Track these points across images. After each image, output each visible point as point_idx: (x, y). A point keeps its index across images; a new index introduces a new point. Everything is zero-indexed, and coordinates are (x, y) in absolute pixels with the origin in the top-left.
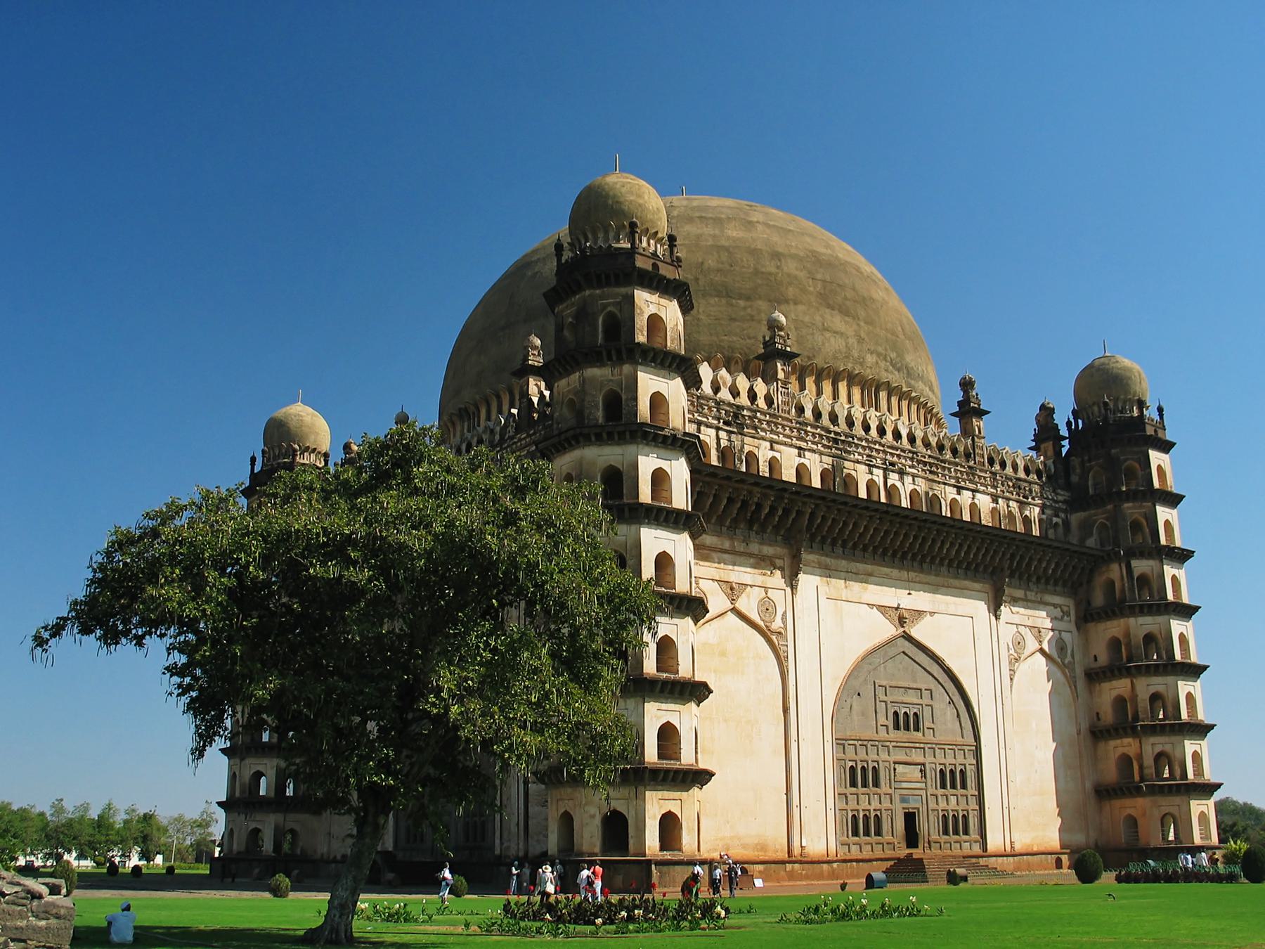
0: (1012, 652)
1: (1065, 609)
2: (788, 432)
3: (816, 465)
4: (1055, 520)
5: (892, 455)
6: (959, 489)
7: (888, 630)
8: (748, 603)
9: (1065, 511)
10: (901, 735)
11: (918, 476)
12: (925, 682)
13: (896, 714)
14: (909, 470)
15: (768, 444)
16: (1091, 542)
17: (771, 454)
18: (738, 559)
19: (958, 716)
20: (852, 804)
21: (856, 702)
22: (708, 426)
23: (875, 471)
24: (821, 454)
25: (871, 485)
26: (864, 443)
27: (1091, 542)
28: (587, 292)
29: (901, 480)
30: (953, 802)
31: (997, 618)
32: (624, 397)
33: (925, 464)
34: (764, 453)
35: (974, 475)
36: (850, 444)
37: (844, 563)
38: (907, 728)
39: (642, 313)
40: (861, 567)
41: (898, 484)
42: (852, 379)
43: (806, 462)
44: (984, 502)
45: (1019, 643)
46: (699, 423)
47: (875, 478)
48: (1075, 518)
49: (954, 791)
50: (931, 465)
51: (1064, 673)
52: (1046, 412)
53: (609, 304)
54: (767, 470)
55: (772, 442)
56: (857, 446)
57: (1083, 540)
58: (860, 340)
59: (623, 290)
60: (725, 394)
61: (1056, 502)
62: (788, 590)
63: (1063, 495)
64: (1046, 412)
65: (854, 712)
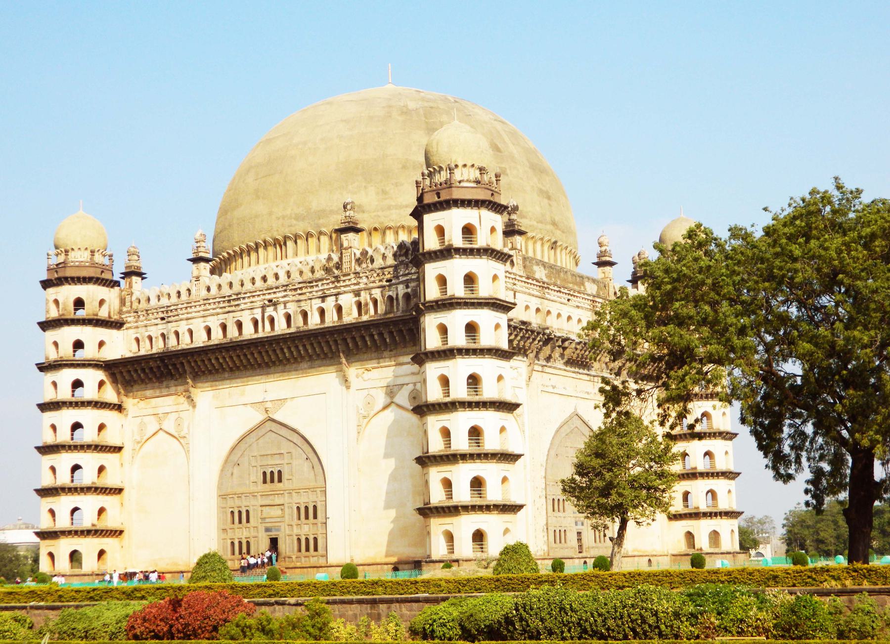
2: (198, 308)
3: (214, 323)
6: (323, 298)
8: (169, 424)
10: (269, 486)
11: (288, 302)
12: (285, 447)
13: (264, 473)
14: (281, 300)
15: (184, 322)
20: (230, 534)
21: (236, 470)
23: (255, 311)
26: (248, 295)
29: (276, 309)
30: (306, 529)
31: (348, 387)
33: (295, 290)
34: (183, 328)
35: (338, 282)
36: (238, 299)
41: (274, 314)
47: (256, 316)
49: (307, 521)
50: (301, 288)
55: (187, 319)
56: (244, 298)
58: (270, 214)
62: (191, 408)
65: (234, 476)
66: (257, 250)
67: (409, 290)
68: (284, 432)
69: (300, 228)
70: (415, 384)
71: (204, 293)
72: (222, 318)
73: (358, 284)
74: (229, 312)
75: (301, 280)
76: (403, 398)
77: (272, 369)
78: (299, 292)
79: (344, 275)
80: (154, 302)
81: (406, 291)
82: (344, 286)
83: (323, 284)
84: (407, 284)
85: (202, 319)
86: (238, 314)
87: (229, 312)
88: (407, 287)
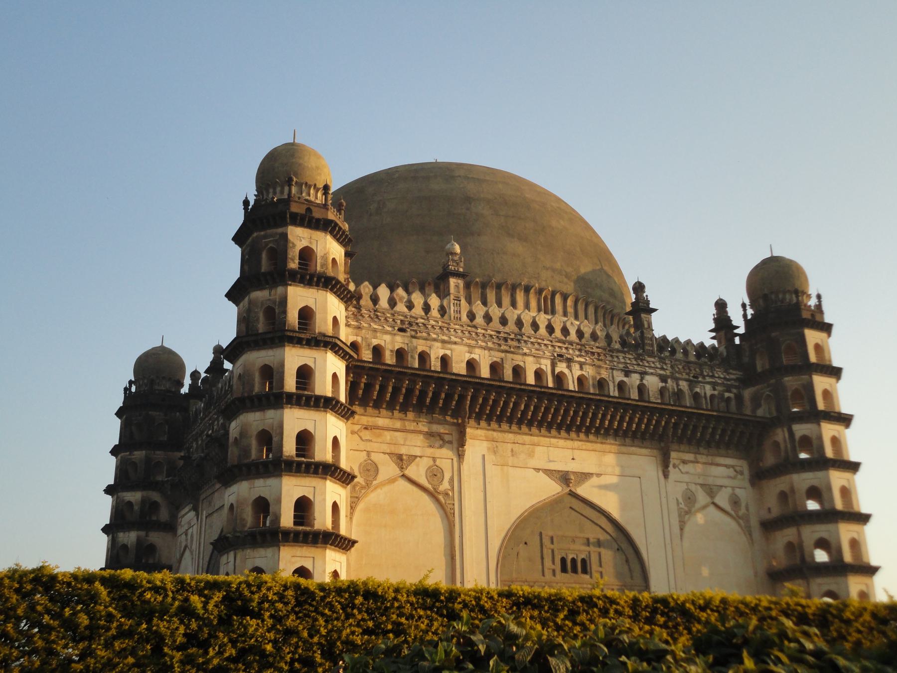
0: (682, 506)
1: (738, 469)
4: (727, 395)
5: (559, 347)
6: (627, 373)
7: (553, 488)
8: (418, 471)
9: (736, 387)
13: (563, 560)
15: (439, 344)
16: (760, 412)
17: (441, 352)
18: (410, 436)
19: (627, 561)
22: (387, 333)
23: (543, 361)
24: (490, 349)
25: (539, 374)
27: (760, 412)
28: (255, 234)
29: (569, 367)
31: (666, 476)
32: (277, 311)
33: (593, 353)
34: (436, 352)
35: (642, 360)
37: (511, 436)
38: (575, 570)
39: (294, 245)
40: (527, 438)
41: (566, 371)
42: (527, 290)
43: (476, 357)
44: (653, 382)
45: (690, 499)
46: (375, 331)
47: (543, 367)
48: (747, 393)
50: (598, 354)
51: (739, 524)
52: (721, 306)
53: (270, 242)
54: (439, 364)
55: (443, 342)
57: (754, 410)
59: (280, 230)
60: (401, 307)
61: (728, 380)
62: (455, 459)
63: (734, 375)
64: (721, 306)
66: (513, 289)
67: (716, 393)
68: (588, 512)
69: (569, 288)
70: (733, 488)
71: (464, 318)
72: (497, 356)
73: (662, 369)
74: (507, 352)
75: (597, 345)
76: (722, 499)
77: (573, 435)
78: (596, 356)
79: (650, 356)
80: (384, 303)
81: (713, 392)
82: (650, 367)
83: (624, 358)
84: (714, 385)
85: (466, 349)
86: (519, 357)
87: (507, 352)
88: (714, 389)
